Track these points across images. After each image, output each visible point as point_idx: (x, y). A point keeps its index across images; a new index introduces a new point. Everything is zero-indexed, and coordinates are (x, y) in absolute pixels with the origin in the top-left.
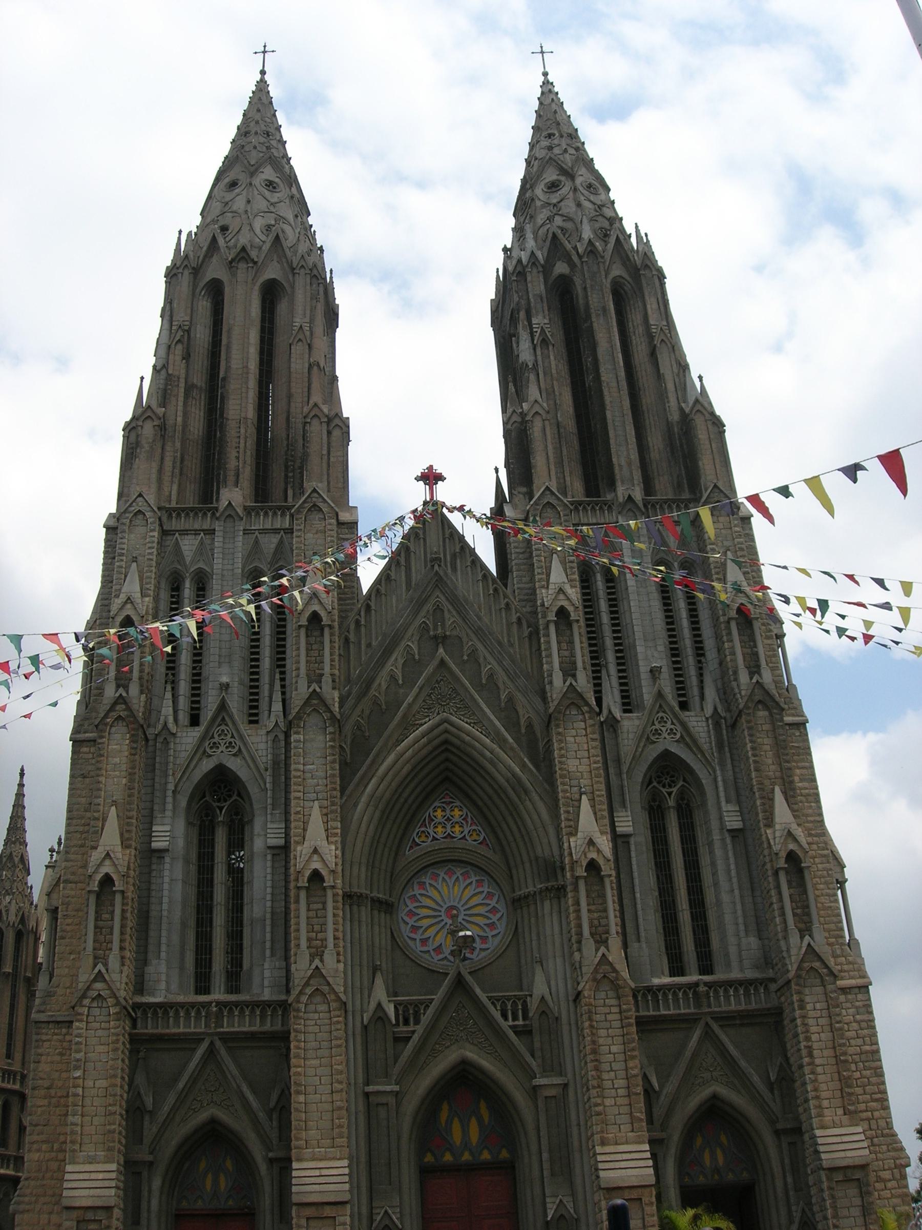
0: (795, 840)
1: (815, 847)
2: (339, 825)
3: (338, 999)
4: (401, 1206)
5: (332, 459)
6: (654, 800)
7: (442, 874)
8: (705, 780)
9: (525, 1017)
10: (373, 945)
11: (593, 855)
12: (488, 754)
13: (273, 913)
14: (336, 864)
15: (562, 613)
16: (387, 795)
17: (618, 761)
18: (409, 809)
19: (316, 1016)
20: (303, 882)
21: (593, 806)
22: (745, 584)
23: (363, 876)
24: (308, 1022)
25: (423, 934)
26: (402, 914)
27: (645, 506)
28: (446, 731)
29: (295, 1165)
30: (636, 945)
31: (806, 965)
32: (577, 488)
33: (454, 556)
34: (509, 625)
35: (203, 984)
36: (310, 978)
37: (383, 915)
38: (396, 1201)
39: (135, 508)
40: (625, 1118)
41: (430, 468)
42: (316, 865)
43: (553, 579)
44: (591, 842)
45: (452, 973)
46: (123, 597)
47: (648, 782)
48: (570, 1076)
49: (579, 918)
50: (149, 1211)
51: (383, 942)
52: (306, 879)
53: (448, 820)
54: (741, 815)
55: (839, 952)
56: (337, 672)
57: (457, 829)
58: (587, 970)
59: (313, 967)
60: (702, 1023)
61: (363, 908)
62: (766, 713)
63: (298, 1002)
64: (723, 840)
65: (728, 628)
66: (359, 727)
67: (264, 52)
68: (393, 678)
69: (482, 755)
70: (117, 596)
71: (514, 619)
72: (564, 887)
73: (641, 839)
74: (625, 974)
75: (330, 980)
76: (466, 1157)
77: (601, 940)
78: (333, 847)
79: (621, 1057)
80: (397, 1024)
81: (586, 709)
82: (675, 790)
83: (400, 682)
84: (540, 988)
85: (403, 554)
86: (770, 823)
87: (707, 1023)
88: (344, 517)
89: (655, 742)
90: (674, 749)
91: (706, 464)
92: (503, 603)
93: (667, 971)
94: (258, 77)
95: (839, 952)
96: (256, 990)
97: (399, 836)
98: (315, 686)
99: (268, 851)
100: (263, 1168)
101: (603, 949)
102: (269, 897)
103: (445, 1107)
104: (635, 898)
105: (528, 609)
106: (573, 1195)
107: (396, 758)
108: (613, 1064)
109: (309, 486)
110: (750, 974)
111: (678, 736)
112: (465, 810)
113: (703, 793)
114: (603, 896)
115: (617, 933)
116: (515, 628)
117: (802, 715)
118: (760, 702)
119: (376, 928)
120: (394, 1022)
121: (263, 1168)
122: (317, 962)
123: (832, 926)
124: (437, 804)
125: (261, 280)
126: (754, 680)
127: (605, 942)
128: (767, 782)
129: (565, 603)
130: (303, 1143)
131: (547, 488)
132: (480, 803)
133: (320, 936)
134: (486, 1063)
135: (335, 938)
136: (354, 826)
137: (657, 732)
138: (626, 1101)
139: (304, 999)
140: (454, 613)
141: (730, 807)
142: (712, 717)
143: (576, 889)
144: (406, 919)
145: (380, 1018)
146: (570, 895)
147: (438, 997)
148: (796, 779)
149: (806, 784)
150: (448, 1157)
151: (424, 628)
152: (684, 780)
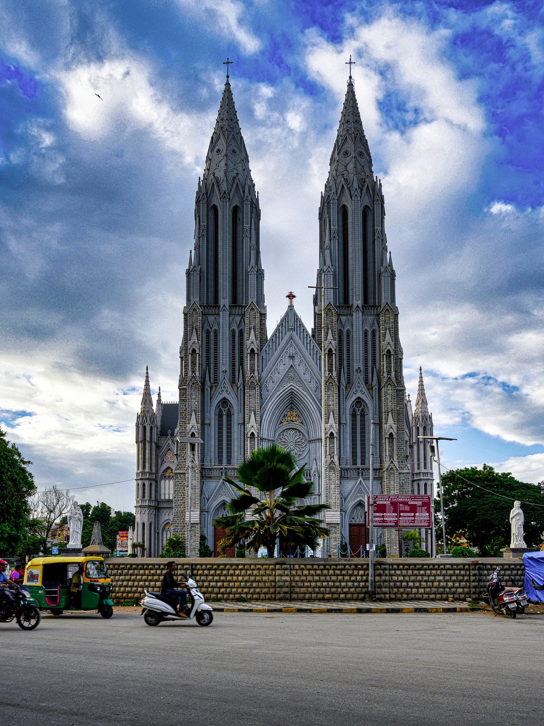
6: (354, 411)
20: (249, 435)
27: (363, 308)
35: (220, 462)
39: (193, 308)
44: (332, 426)
46: (192, 341)
57: (294, 418)
65: (383, 357)
70: (190, 340)
88: (263, 312)
98: (252, 374)
113: (368, 410)
114: (333, 443)
117: (403, 386)
129: (332, 347)
137: (357, 391)
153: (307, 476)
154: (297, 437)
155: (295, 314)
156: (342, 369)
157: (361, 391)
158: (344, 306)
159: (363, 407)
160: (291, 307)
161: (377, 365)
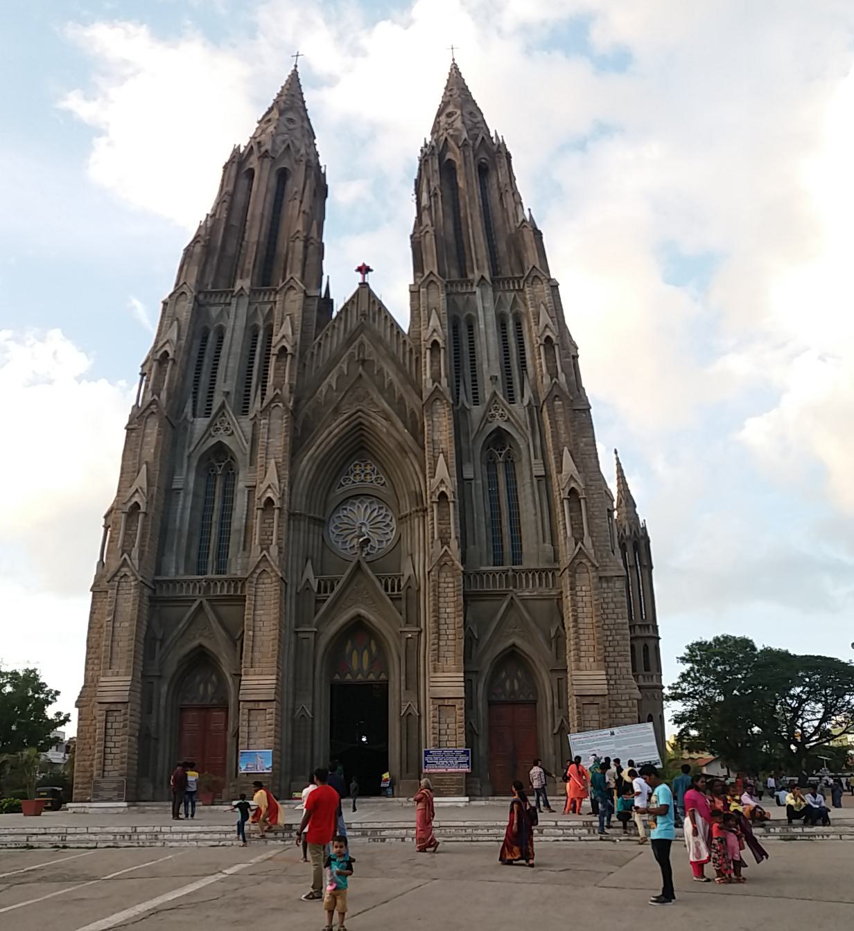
0: (576, 481)
1: (593, 488)
2: (287, 472)
3: (277, 575)
4: (313, 704)
5: (307, 262)
7: (358, 504)
8: (523, 446)
9: (399, 590)
10: (308, 545)
11: (443, 489)
12: (385, 430)
13: (246, 527)
14: (283, 495)
15: (435, 343)
16: (321, 456)
17: (468, 435)
18: (336, 466)
19: (263, 586)
21: (446, 461)
22: (551, 323)
23: (304, 503)
24: (258, 590)
25: (344, 539)
26: (332, 528)
27: (493, 282)
28: (360, 417)
29: (243, 678)
30: (472, 547)
31: (577, 561)
32: (455, 275)
33: (374, 314)
34: (404, 354)
36: (260, 562)
37: (317, 527)
38: (310, 701)
40: (451, 654)
41: (364, 265)
42: (269, 494)
43: (431, 324)
45: (355, 561)
47: (486, 446)
48: (422, 626)
49: (433, 528)
50: (159, 705)
51: (316, 544)
52: (262, 503)
53: (363, 472)
54: (545, 466)
55: (605, 555)
56: (295, 382)
57: (368, 477)
58: (435, 559)
59: (262, 555)
60: (509, 597)
61: (302, 523)
62: (560, 403)
63: (252, 577)
64: (532, 483)
66: (307, 415)
67: (297, 56)
68: (330, 386)
69: (381, 431)
71: (408, 349)
72: (427, 509)
73: (479, 482)
74: (458, 563)
75: (272, 563)
76: (360, 677)
77: (444, 541)
78: (282, 485)
79: (453, 615)
80: (319, 591)
81: (445, 401)
82: (504, 452)
83: (334, 388)
84: (407, 571)
85: (344, 313)
86: (560, 472)
87: (512, 598)
89: (491, 422)
90: (504, 426)
91: (531, 258)
92: (401, 340)
93: (492, 563)
94: (293, 68)
95: (605, 555)
96: (233, 572)
97: (330, 481)
98: (278, 391)
99: (247, 490)
100: (230, 680)
101: (446, 547)
102: (244, 517)
103: (349, 643)
104: (473, 517)
105: (418, 343)
106: (419, 702)
107: (329, 433)
108: (447, 620)
109: (288, 277)
110: (541, 566)
111: (506, 418)
112: (373, 466)
113: (520, 453)
115: (457, 538)
116: (408, 355)
117: (589, 405)
118: (557, 396)
119: (311, 535)
120: (316, 590)
121: (230, 680)
122: (265, 552)
123: (602, 539)
124: (356, 462)
125: (277, 168)
126: (553, 382)
127: (448, 544)
128: (560, 445)
129: (437, 338)
130: (248, 665)
131: (431, 273)
132: (381, 460)
133: (270, 538)
134: (372, 618)
135: (279, 539)
136: (299, 474)
137: (493, 416)
138: (452, 643)
139: (255, 576)
140: (371, 346)
141: (537, 461)
142: (528, 406)
143: (433, 511)
144: (334, 530)
145: (308, 589)
146: (429, 514)
147: (345, 577)
148: (582, 445)
149: (590, 448)
150: (349, 677)
151: (352, 355)
152: (510, 446)
153: (393, 590)
154: (375, 514)
155: (371, 293)
156: (461, 383)
157: (502, 416)
158: (459, 282)
159: (508, 448)
160: (364, 285)
161: (530, 369)
